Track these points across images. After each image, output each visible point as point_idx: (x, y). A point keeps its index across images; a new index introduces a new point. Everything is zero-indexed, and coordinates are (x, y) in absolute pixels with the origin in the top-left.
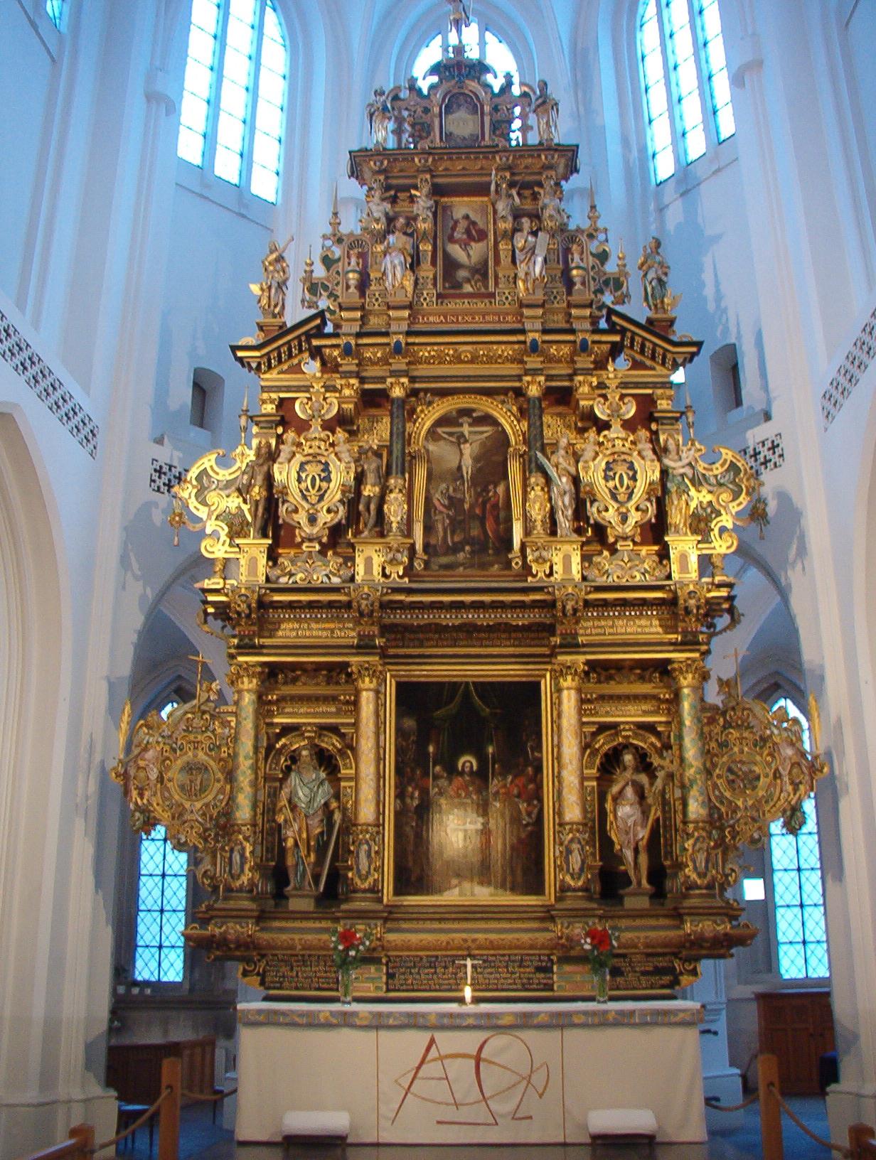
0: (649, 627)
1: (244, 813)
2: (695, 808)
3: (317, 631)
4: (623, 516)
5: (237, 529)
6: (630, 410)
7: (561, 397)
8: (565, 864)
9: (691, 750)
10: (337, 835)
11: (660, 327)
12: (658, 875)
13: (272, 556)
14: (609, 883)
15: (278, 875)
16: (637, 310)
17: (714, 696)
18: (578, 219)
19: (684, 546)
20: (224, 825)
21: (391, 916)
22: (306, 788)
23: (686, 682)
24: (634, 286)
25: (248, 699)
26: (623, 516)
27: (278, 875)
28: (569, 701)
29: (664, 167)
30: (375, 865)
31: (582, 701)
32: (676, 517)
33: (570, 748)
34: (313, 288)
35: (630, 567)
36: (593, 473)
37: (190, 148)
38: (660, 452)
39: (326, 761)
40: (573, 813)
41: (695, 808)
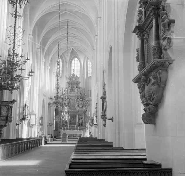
6: (82, 100)
8: (77, 124)
13: (63, 108)
14: (80, 125)
18: (80, 86)
19: (84, 108)
26: (81, 106)
27: (63, 124)
30: (68, 124)
31: (78, 116)
32: (84, 106)
33: (78, 118)
34: (65, 91)
35: (81, 109)
36: (80, 103)
41: (84, 121)
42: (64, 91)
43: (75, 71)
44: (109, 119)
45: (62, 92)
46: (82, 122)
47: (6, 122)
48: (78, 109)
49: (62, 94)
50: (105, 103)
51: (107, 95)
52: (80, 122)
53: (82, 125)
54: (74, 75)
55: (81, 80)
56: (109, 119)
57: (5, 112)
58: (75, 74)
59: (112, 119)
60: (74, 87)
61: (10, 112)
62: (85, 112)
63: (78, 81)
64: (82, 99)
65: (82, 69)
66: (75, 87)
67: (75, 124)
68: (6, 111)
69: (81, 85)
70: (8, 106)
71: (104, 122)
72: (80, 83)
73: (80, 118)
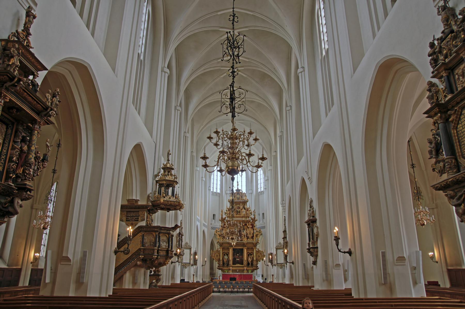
0: (252, 245)
1: (221, 259)
2: (255, 259)
3: (227, 245)
4: (250, 236)
5: (220, 235)
6: (251, 226)
7: (246, 225)
9: (255, 254)
10: (228, 261)
11: (254, 218)
12: (252, 264)
14: (248, 264)
15: (224, 264)
16: (253, 217)
17: (257, 250)
18: (248, 207)
20: (219, 260)
21: (232, 267)
22: (226, 257)
23: (255, 249)
24: (253, 213)
25: (221, 251)
26: (250, 236)
27: (224, 264)
28: (246, 251)
29: (259, 191)
30: (231, 263)
32: (255, 236)
34: (225, 213)
35: (250, 240)
36: (248, 232)
37: (212, 190)
38: (253, 230)
39: (227, 255)
40: (246, 259)
41: (255, 259)
42: (224, 214)
43: (240, 183)
44: (345, 252)
45: (222, 216)
46: (252, 261)
47: (166, 259)
48: (245, 240)
49: (222, 218)
50: (315, 228)
51: (317, 217)
52: (250, 260)
53: (252, 264)
54: (238, 190)
55: (248, 198)
56: (345, 252)
57: (165, 244)
58: (240, 188)
59: (350, 253)
60: (239, 208)
61: (170, 243)
62: (255, 245)
63: (244, 198)
64: (251, 225)
65: (249, 182)
66: (241, 207)
67: (241, 262)
68: (166, 242)
69: (248, 206)
70: (169, 234)
71: (312, 259)
72: (247, 201)
73: (249, 255)
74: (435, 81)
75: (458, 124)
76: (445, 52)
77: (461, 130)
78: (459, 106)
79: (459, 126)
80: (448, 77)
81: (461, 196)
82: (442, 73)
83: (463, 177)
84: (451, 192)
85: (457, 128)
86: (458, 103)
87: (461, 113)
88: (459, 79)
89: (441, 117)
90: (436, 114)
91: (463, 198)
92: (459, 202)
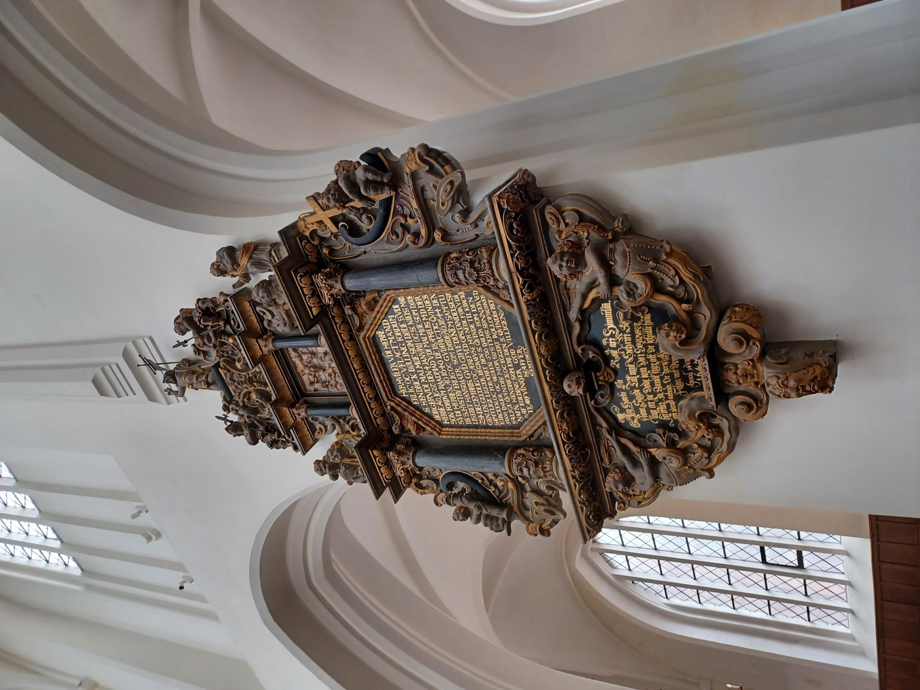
74: (319, 451)
75: (430, 417)
76: (254, 396)
77: (448, 413)
78: (386, 400)
79: (437, 417)
80: (311, 406)
81: (625, 450)
82: (299, 418)
83: (562, 415)
84: (609, 479)
85: (440, 423)
86: (377, 398)
87: (403, 399)
88: (325, 384)
89: (400, 453)
90: (388, 463)
91: (630, 445)
92: (643, 460)
